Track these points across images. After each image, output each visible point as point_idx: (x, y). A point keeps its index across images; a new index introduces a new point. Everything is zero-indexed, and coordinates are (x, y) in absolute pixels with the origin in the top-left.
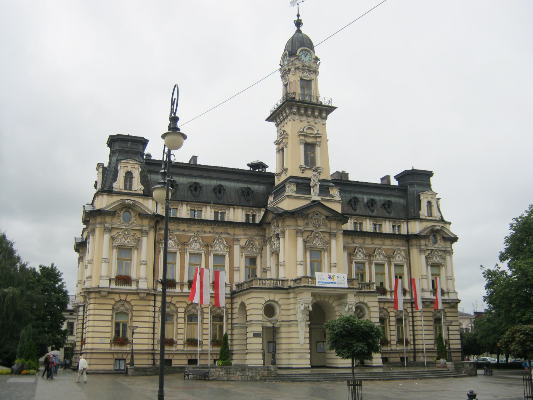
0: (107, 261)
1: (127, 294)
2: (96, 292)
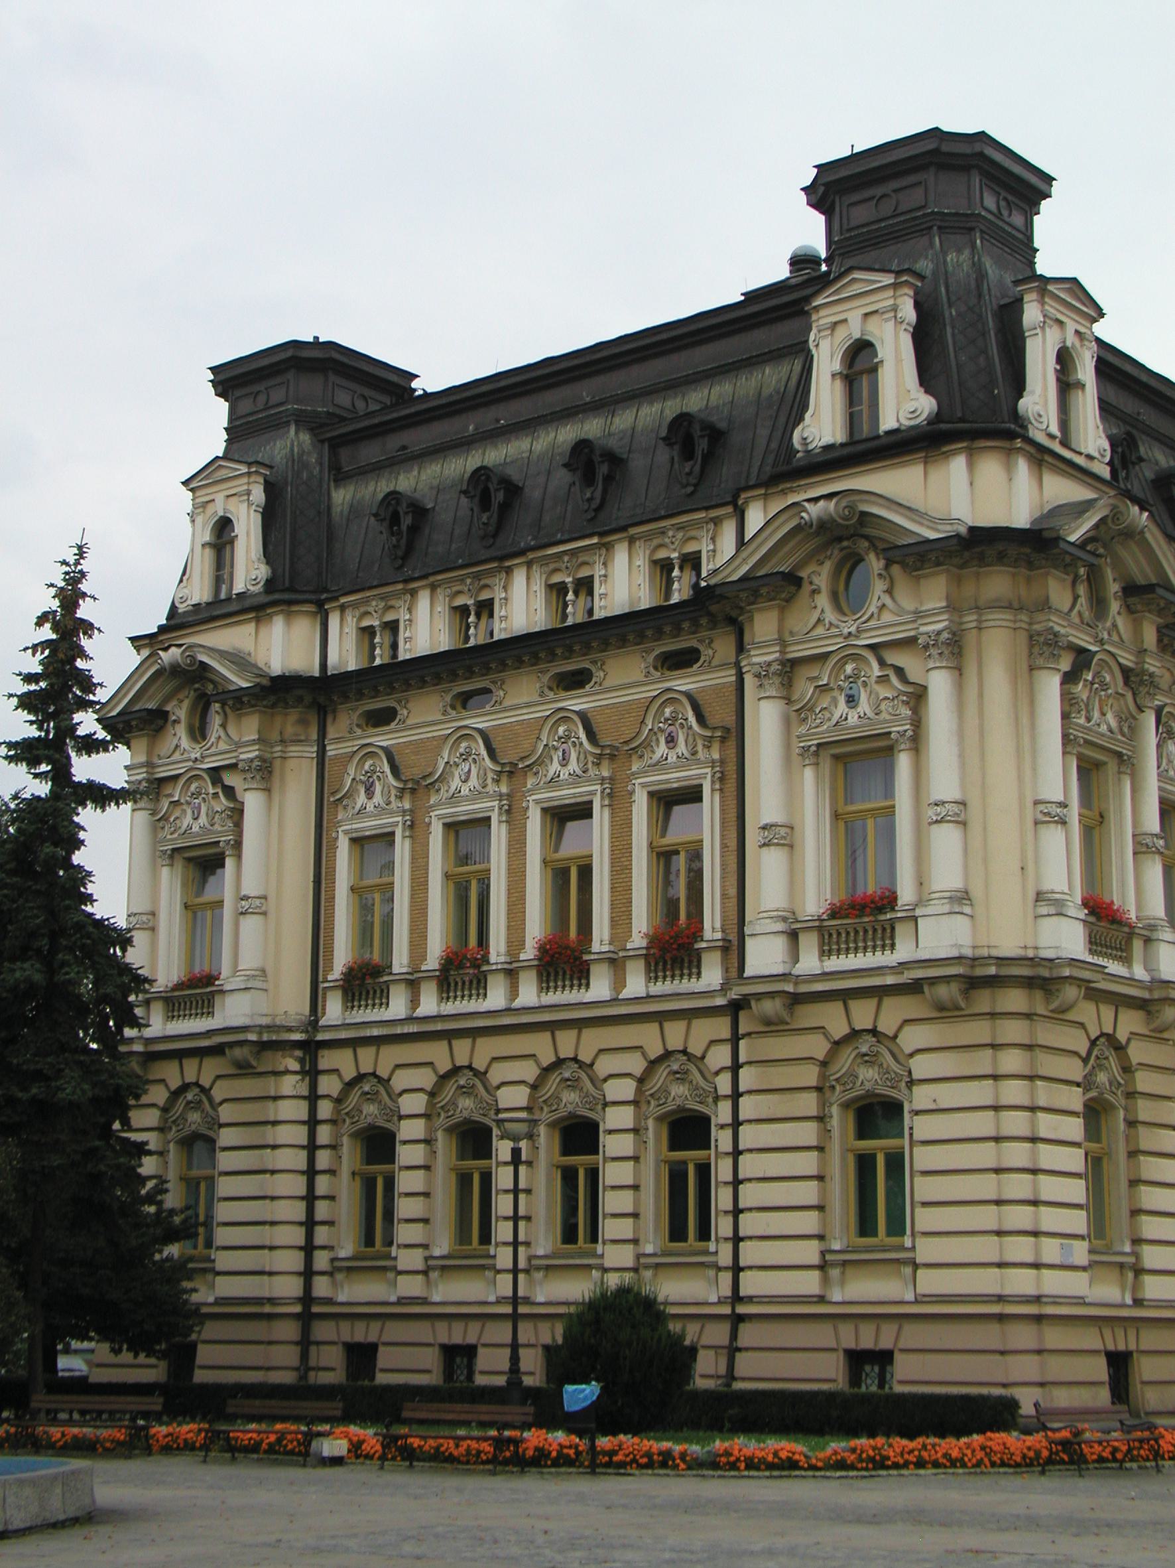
0: (1050, 815)
1: (1120, 1001)
2: (1030, 983)
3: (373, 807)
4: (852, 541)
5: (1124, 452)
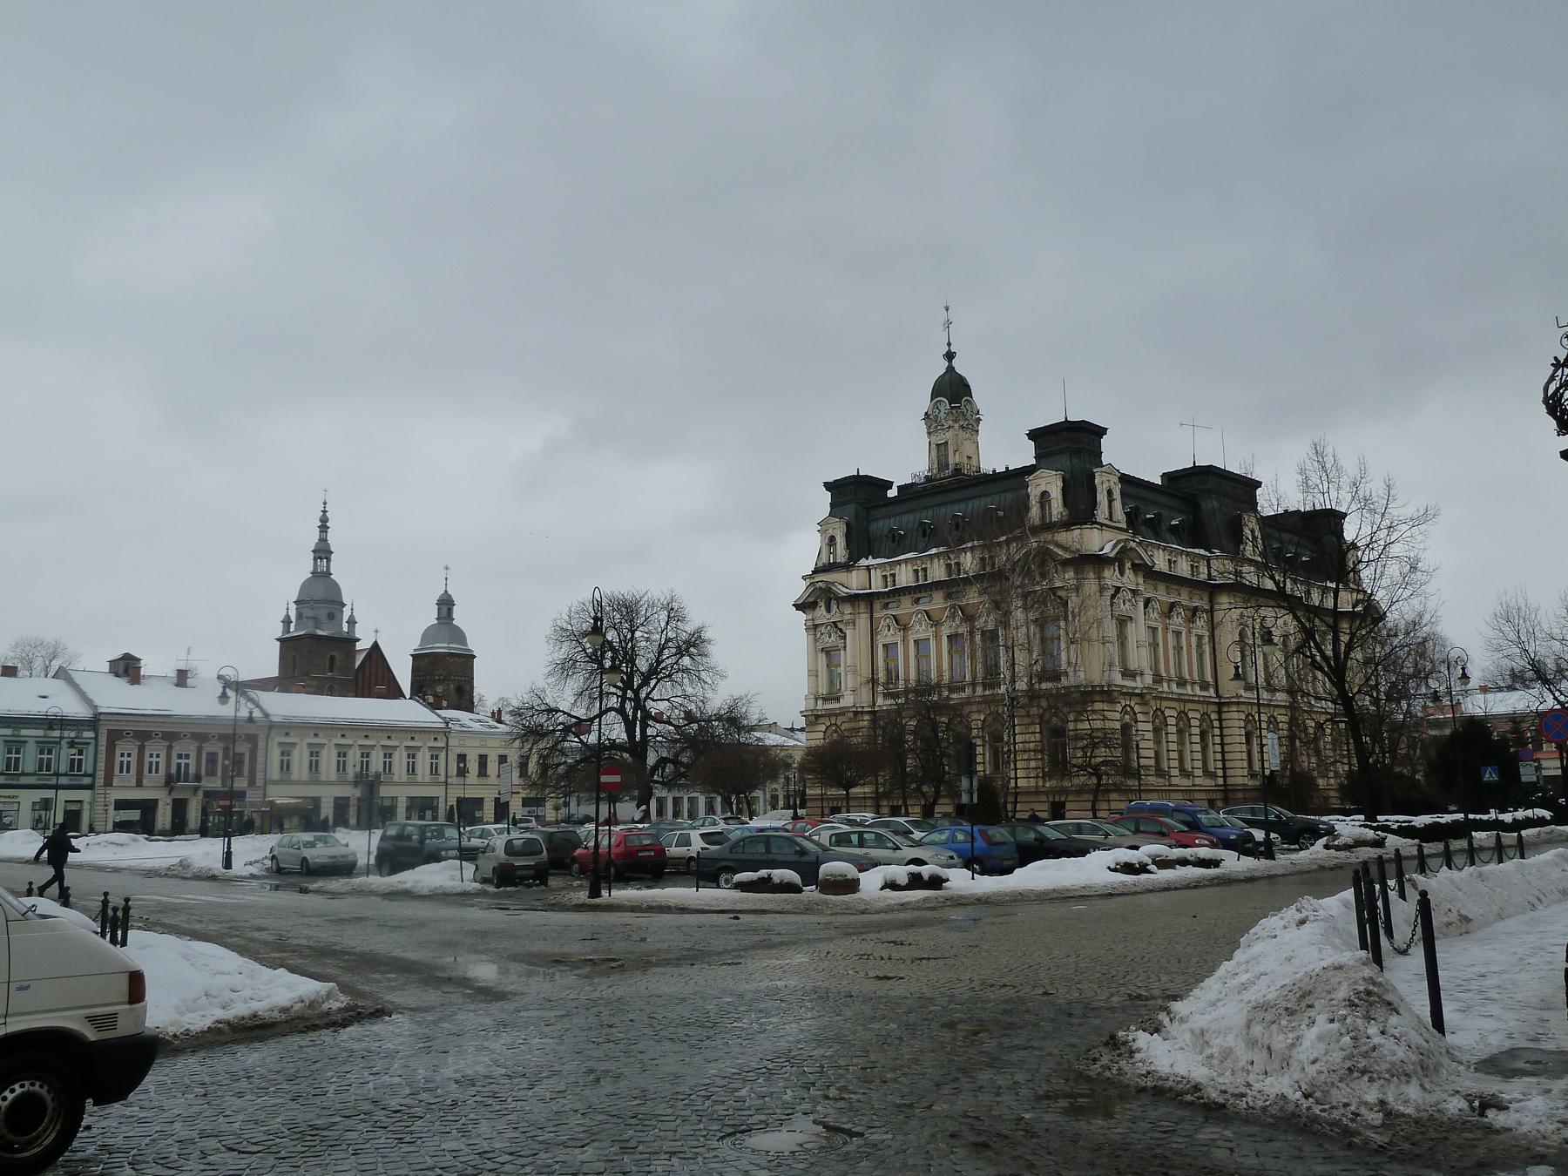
3: (888, 635)
4: (1044, 556)
5: (1132, 518)
